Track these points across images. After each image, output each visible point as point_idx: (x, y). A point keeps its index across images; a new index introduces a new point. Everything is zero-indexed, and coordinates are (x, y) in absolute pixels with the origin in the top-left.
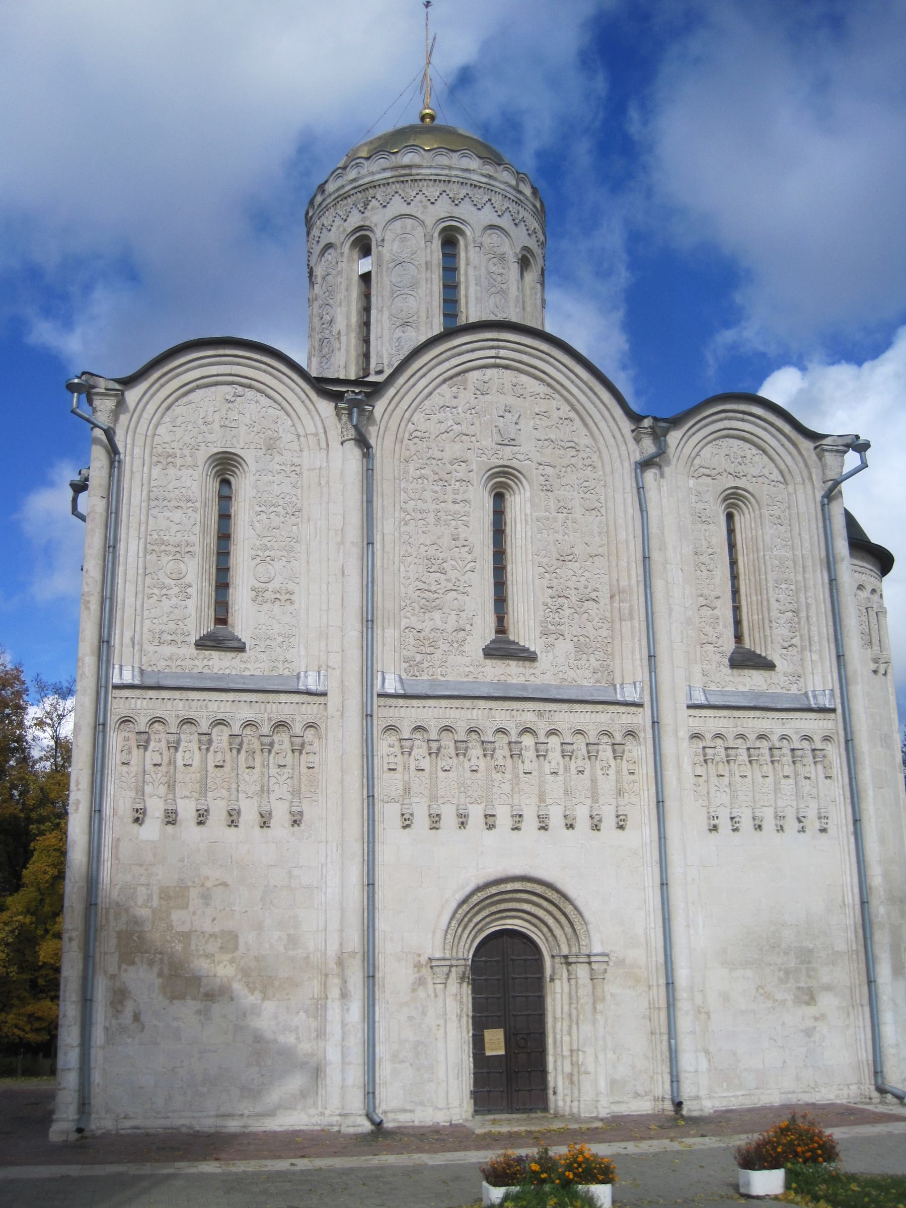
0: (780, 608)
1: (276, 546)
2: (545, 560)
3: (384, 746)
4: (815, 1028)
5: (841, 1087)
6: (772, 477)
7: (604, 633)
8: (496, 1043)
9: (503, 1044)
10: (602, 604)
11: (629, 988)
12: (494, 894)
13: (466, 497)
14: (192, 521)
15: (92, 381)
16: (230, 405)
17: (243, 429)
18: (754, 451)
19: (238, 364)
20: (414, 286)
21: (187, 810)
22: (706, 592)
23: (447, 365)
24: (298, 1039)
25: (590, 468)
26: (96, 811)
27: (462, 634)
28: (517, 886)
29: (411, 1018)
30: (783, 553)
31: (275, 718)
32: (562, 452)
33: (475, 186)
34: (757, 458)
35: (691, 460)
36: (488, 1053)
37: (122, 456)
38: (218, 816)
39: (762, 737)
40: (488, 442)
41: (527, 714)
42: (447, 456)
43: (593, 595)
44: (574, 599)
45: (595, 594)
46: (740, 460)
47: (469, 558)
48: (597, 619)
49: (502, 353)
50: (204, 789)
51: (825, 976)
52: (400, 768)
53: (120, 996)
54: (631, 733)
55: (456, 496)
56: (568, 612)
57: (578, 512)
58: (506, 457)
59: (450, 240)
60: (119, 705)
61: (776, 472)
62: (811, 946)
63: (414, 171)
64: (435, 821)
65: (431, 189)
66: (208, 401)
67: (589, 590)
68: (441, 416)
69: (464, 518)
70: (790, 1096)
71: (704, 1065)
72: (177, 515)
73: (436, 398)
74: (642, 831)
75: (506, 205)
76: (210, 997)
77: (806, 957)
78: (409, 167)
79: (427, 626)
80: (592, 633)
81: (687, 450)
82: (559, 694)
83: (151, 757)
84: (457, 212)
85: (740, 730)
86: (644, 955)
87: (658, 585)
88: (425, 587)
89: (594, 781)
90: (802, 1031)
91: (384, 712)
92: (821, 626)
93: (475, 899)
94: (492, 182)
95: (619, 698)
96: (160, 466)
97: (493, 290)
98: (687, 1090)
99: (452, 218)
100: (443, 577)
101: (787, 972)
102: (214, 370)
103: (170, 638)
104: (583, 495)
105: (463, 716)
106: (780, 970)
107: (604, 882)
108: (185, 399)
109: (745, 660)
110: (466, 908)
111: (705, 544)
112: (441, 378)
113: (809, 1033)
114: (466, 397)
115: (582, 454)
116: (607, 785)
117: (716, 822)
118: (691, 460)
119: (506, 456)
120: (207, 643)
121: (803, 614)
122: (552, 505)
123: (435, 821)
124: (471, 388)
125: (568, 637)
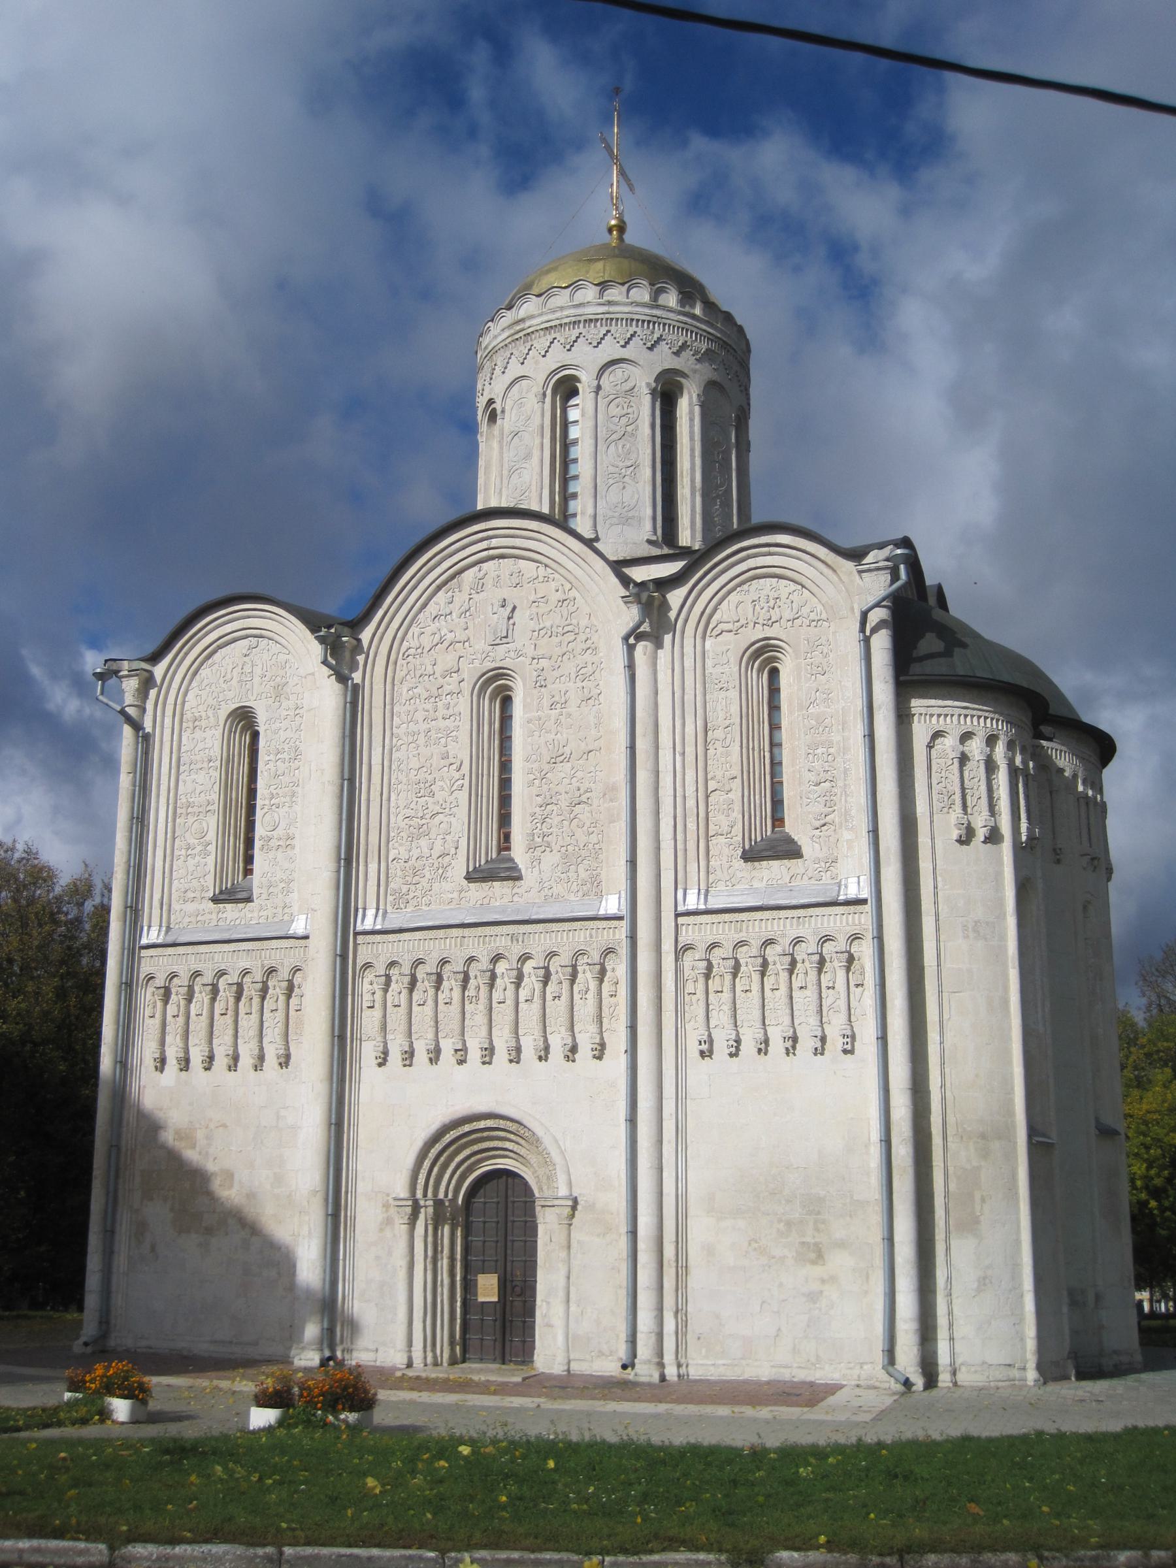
0: (813, 778)
1: (280, 791)
2: (535, 766)
4: (821, 1292)
5: (852, 1365)
6: (813, 616)
7: (594, 838)
8: (488, 1288)
9: (496, 1290)
10: (595, 805)
11: (598, 1235)
13: (456, 710)
14: (213, 780)
15: (114, 666)
16: (246, 659)
17: (257, 680)
18: (793, 586)
19: (249, 617)
20: (528, 457)
21: (197, 1056)
22: (719, 774)
23: (439, 570)
24: (279, 1273)
25: (589, 651)
27: (447, 859)
28: (489, 1123)
29: (378, 1258)
30: (822, 709)
31: (268, 963)
32: (560, 638)
33: (591, 320)
34: (794, 597)
36: (481, 1299)
37: (148, 729)
39: (769, 942)
40: (481, 645)
41: (500, 939)
42: (439, 669)
43: (584, 798)
44: (564, 804)
45: (588, 795)
46: (771, 603)
47: (457, 775)
48: (588, 824)
49: (494, 542)
52: (377, 1005)
53: (141, 1228)
54: (609, 951)
55: (445, 712)
56: (556, 820)
57: (572, 708)
58: (498, 659)
61: (820, 607)
62: (822, 1193)
63: (528, 324)
64: (409, 1056)
65: (543, 340)
67: (582, 791)
68: (433, 627)
69: (454, 733)
70: (782, 1370)
72: (201, 777)
73: (432, 608)
74: (616, 1061)
75: (634, 328)
76: (209, 1231)
77: (815, 1207)
78: (522, 320)
79: (415, 853)
80: (583, 839)
82: (537, 913)
83: (171, 1009)
84: (568, 358)
85: (742, 936)
88: (412, 813)
90: (804, 1294)
93: (448, 1138)
94: (612, 309)
95: (602, 912)
96: (189, 731)
97: (614, 437)
99: (564, 367)
100: (430, 800)
101: (789, 1224)
103: (193, 895)
104: (580, 684)
105: (432, 948)
106: (780, 1221)
108: (210, 661)
110: (438, 1147)
111: (721, 715)
112: (434, 586)
113: (813, 1297)
114: (461, 598)
115: (582, 637)
116: (585, 1009)
117: (704, 1047)
118: (707, 618)
121: (840, 783)
122: (546, 703)
124: (466, 588)
125: (555, 848)
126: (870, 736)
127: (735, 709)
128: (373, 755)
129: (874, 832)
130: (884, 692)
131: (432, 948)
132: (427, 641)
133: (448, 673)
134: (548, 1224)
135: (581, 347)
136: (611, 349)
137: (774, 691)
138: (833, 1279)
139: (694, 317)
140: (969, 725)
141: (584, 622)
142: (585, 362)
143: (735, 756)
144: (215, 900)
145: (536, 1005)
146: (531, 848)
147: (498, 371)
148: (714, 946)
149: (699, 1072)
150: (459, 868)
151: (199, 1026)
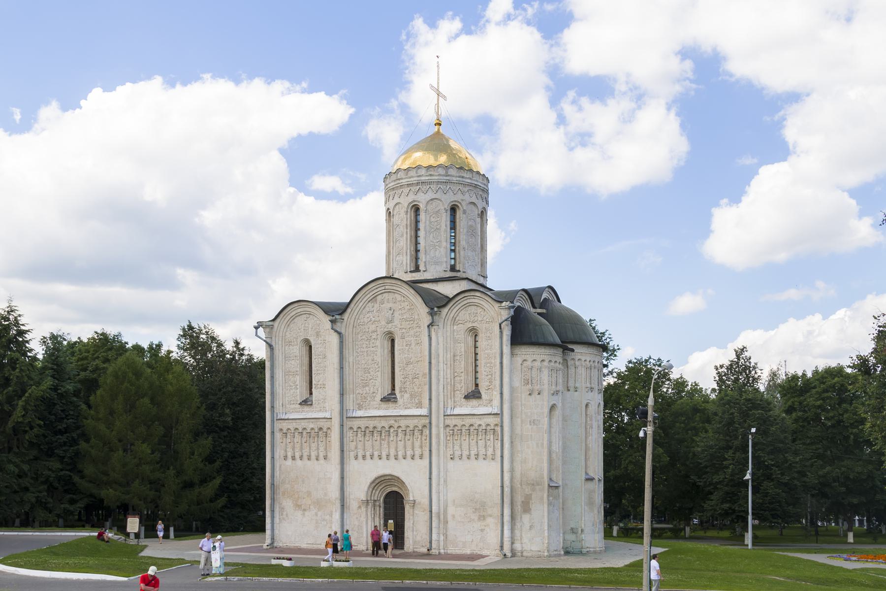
3: (349, 435)
12: (380, 481)
20: (402, 236)
26: (273, 458)
35: (454, 319)
38: (305, 457)
40: (383, 323)
42: (370, 330)
50: (301, 449)
51: (490, 512)
53: (282, 509)
54: (424, 426)
57: (413, 345)
59: (416, 209)
60: (278, 425)
64: (364, 457)
66: (299, 321)
71: (442, 538)
72: (293, 362)
73: (367, 309)
76: (304, 510)
77: (483, 505)
81: (452, 315)
86: (426, 501)
87: (433, 372)
89: (413, 443)
91: (349, 423)
92: (498, 382)
98: (434, 546)
99: (414, 201)
102: (299, 310)
107: (414, 479)
109: (474, 394)
113: (482, 530)
114: (377, 306)
116: (417, 444)
118: (454, 319)
119: (390, 327)
120: (306, 402)
123: (364, 457)
126: (501, 363)
127: (463, 350)
128: (350, 358)
129: (502, 394)
130: (507, 349)
131: (371, 424)
132: (366, 320)
133: (374, 332)
134: (407, 508)
135: (420, 194)
136: (430, 195)
137: (476, 341)
138: (488, 525)
139: (463, 177)
140: (534, 357)
141: (416, 317)
142: (422, 199)
143: (462, 366)
144: (300, 404)
145: (403, 442)
146: (401, 392)
147: (391, 198)
148: (456, 425)
149: (451, 464)
150: (379, 397)
151: (298, 446)
